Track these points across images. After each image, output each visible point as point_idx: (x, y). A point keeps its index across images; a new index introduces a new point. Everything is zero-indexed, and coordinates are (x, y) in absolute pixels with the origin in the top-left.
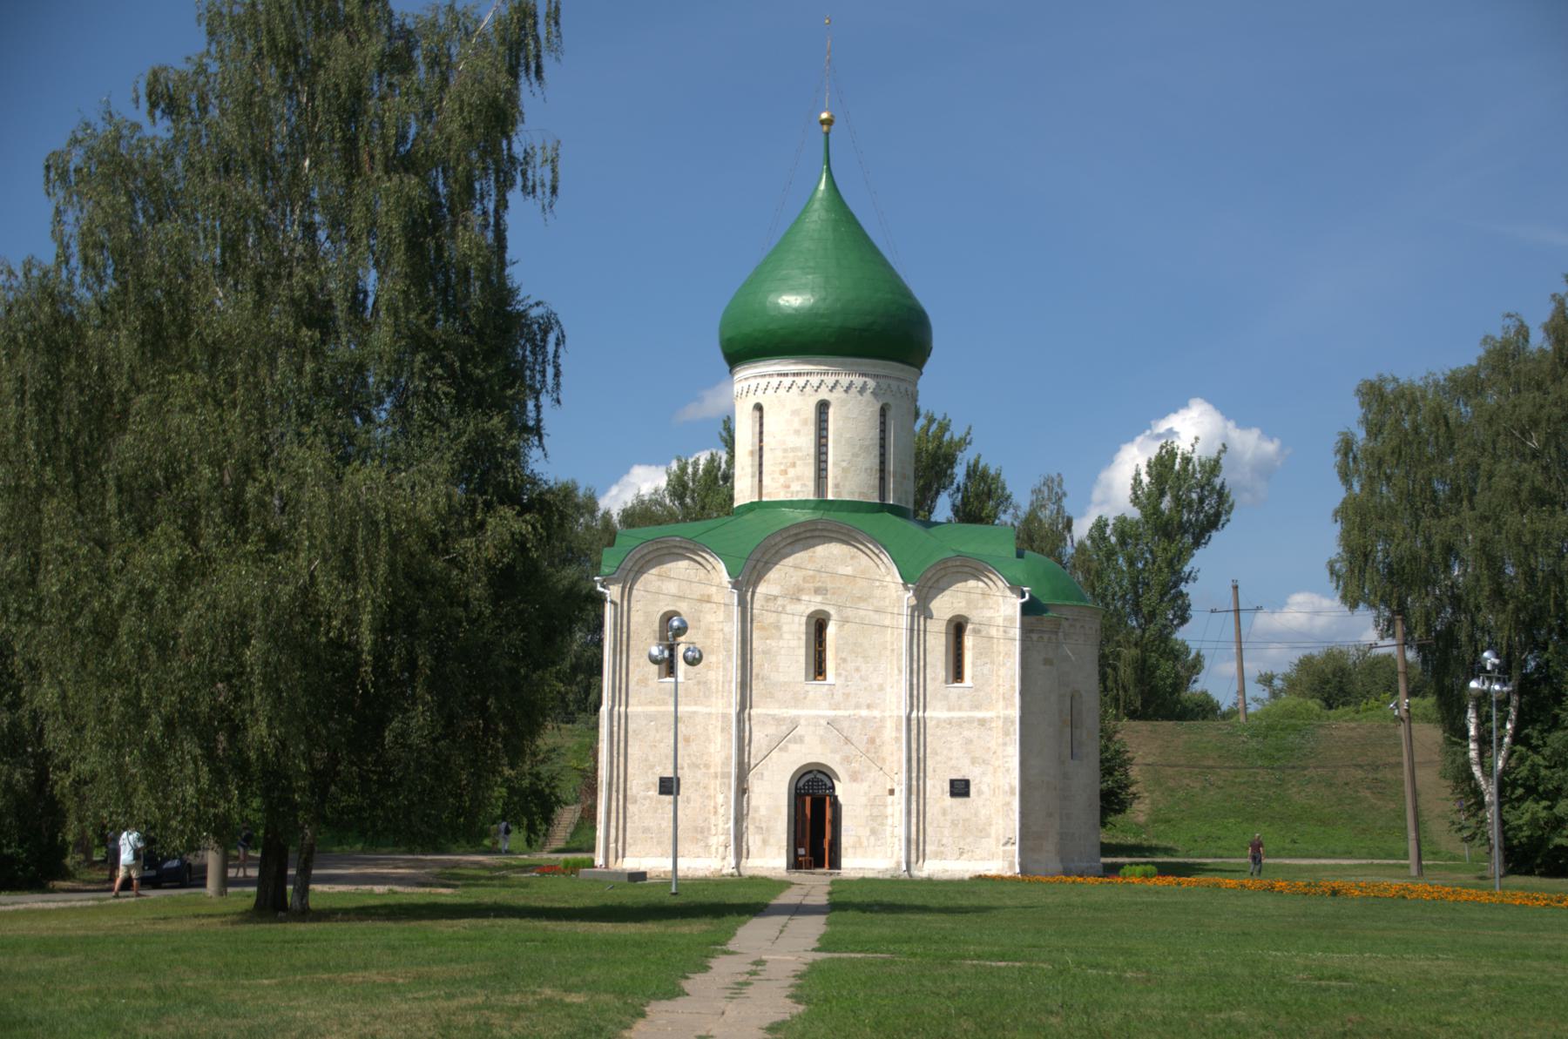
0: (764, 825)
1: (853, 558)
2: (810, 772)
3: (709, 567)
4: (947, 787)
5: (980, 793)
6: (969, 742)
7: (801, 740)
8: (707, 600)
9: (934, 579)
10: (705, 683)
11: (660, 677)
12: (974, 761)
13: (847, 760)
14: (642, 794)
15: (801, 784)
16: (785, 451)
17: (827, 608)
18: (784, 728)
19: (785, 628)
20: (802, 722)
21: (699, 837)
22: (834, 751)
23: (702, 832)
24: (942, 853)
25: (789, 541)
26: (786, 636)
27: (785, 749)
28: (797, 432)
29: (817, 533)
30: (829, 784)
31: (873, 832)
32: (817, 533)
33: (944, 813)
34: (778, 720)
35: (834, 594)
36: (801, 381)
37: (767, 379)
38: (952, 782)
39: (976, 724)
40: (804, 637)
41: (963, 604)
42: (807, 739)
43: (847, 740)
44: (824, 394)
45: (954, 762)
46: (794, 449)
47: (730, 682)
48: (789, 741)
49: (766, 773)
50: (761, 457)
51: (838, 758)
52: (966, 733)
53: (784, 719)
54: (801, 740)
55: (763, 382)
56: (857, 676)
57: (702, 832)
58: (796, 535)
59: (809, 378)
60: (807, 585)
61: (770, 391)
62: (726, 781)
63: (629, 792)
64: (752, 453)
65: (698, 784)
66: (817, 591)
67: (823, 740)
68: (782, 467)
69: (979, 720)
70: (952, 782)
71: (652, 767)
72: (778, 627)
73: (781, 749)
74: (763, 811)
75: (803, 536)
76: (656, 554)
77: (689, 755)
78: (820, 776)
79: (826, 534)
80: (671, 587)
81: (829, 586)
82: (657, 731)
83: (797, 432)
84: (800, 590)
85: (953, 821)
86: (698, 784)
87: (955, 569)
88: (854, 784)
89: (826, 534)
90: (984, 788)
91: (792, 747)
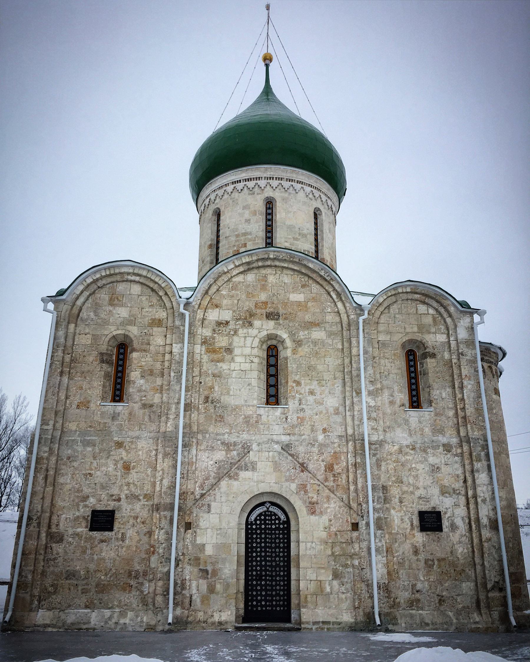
0: (210, 568)
1: (303, 286)
2: (262, 504)
3: (161, 293)
4: (416, 522)
5: (453, 527)
6: (435, 469)
7: (253, 467)
8: (159, 323)
9: (386, 304)
10: (151, 406)
11: (103, 399)
12: (444, 492)
13: (303, 487)
14: (71, 531)
15: (253, 518)
16: (237, 236)
17: (279, 333)
18: (235, 453)
19: (237, 351)
20: (255, 447)
21: (132, 583)
22: (290, 479)
23: (136, 577)
24: (418, 600)
25: (241, 269)
26: (238, 359)
27: (235, 477)
28: (248, 221)
29: (269, 263)
30: (283, 517)
31: (336, 575)
32: (269, 263)
33: (416, 552)
34: (228, 446)
35: (286, 319)
36: (251, 184)
37: (224, 188)
38: (422, 514)
39: (441, 448)
40: (256, 360)
41: (416, 329)
42: (259, 465)
43: (303, 467)
44: (269, 193)
45: (421, 492)
46: (245, 234)
47: (178, 403)
48: (240, 468)
49: (213, 504)
50: (218, 248)
51: (293, 486)
52: (432, 460)
53: (235, 444)
54: (253, 467)
55: (220, 192)
56: (311, 398)
57: (136, 577)
58: (248, 263)
59: (258, 181)
60: (259, 311)
61: (226, 196)
62: (168, 514)
63: (54, 529)
64: (210, 246)
65: (136, 518)
66: (270, 316)
67: (277, 467)
68: (235, 248)
69: (444, 445)
70: (422, 514)
71: (85, 498)
72: (229, 350)
73: (230, 477)
74: (209, 551)
75: (255, 265)
76: (109, 280)
77: (128, 484)
78: (273, 509)
79: (277, 263)
80: (123, 312)
81: (281, 311)
82: (95, 458)
83: (248, 221)
84: (252, 315)
85: (426, 561)
86: (136, 518)
87: (405, 296)
88: (313, 518)
89: (277, 263)
90: (459, 522)
91: (243, 474)
